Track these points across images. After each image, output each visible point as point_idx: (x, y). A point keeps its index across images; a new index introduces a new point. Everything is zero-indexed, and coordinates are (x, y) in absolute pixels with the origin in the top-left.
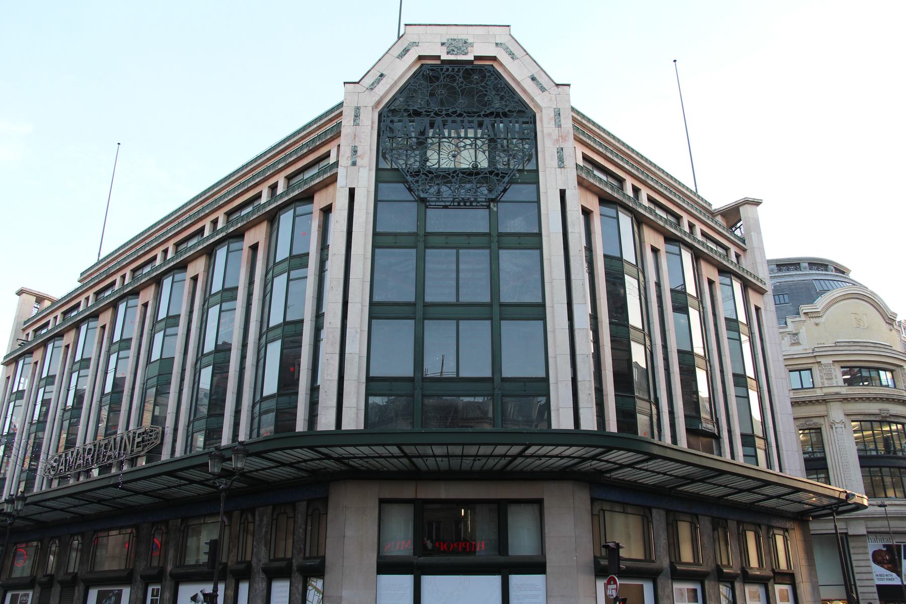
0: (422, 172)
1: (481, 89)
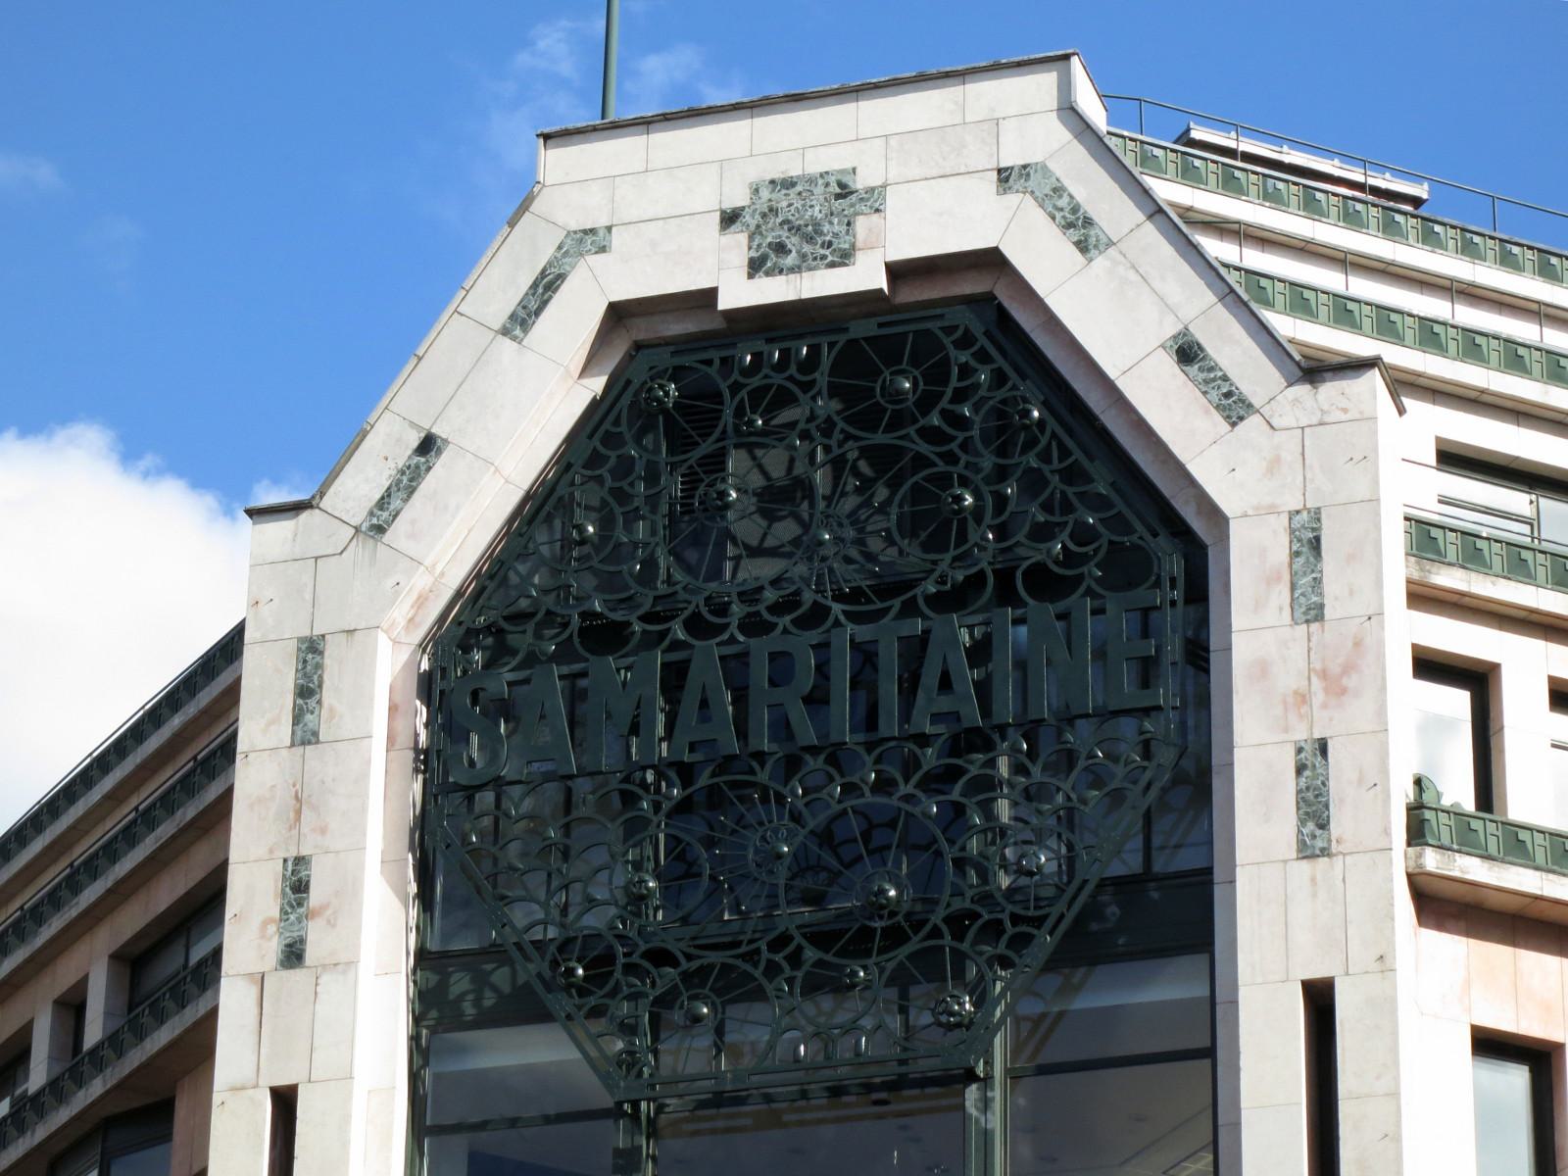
0: (621, 960)
1: (924, 448)
